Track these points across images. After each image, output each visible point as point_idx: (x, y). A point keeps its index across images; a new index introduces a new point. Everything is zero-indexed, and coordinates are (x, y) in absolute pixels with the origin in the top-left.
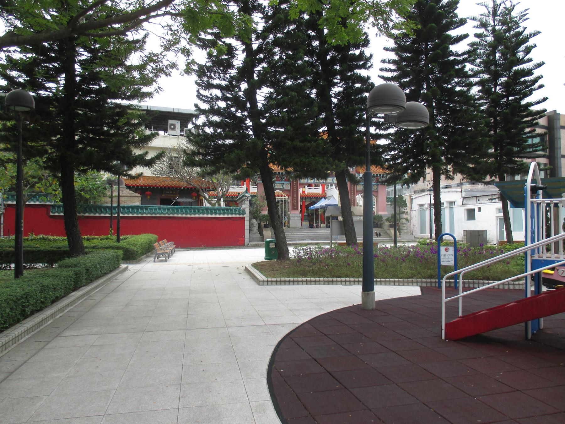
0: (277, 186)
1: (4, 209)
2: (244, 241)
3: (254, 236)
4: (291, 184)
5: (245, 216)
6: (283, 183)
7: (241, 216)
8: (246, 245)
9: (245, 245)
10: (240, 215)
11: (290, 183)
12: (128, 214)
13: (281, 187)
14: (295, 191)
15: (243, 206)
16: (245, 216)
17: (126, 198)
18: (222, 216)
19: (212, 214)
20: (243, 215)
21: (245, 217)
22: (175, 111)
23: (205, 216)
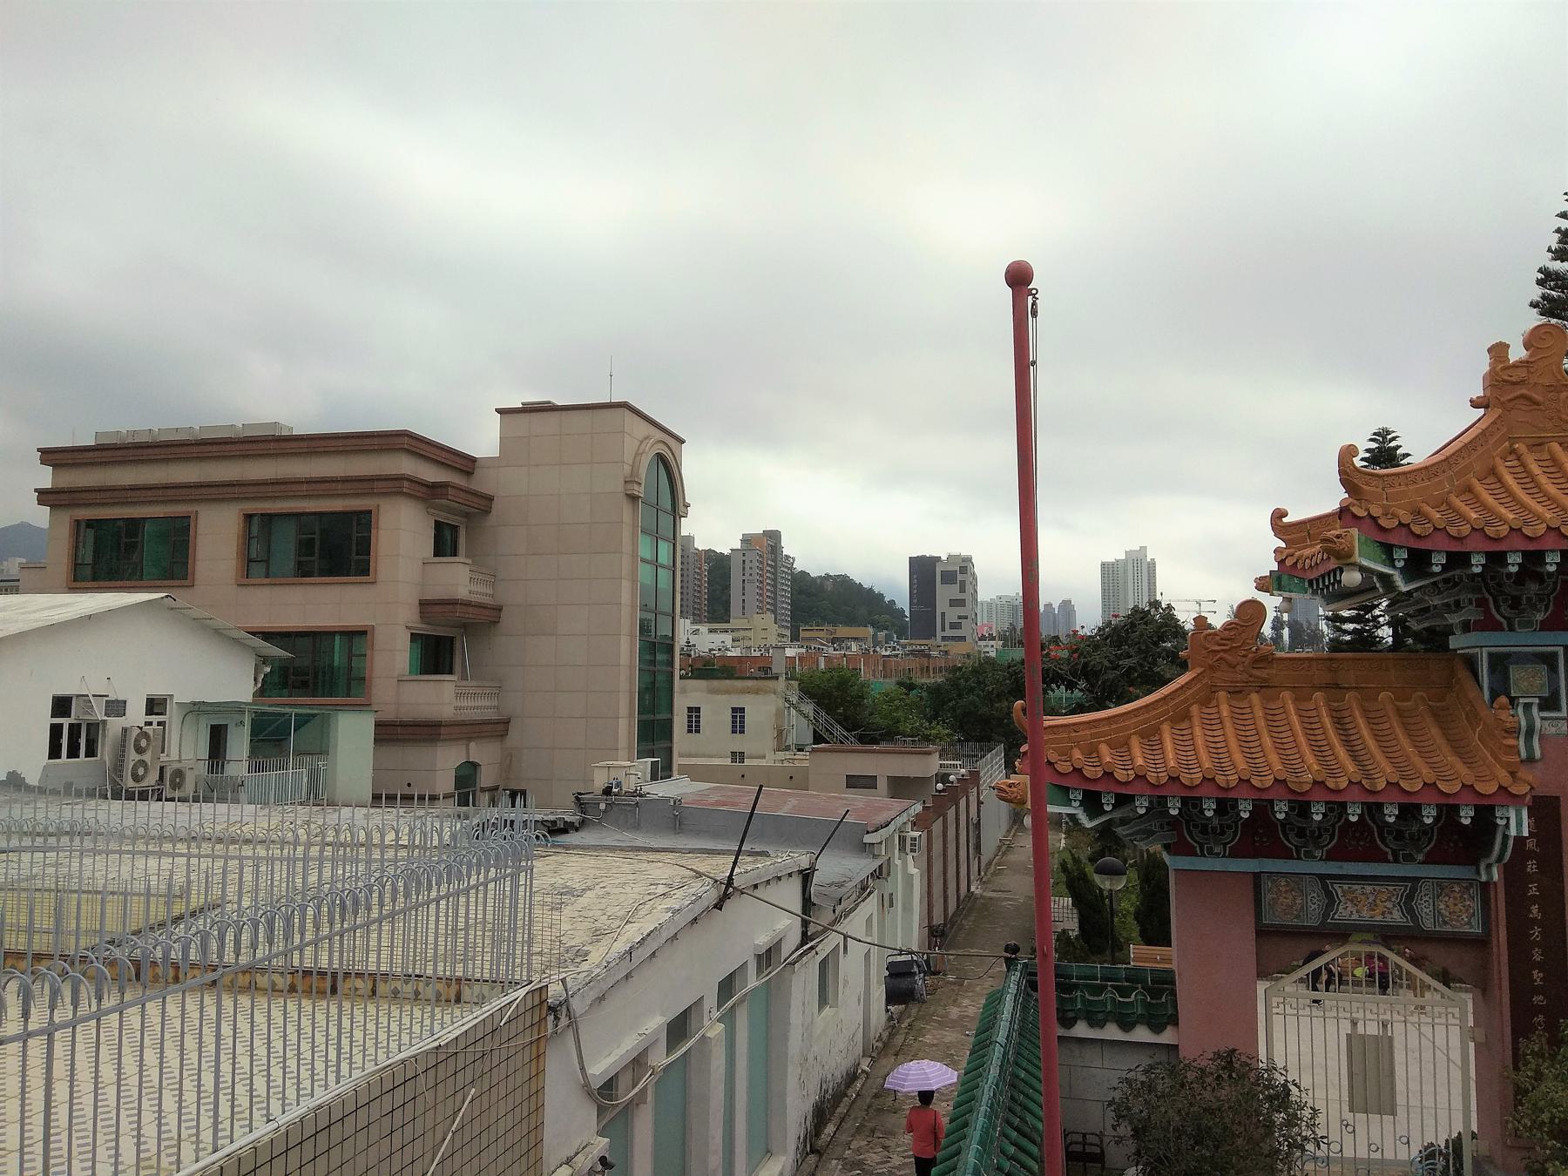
11: (1486, 887)
13: (1397, 917)
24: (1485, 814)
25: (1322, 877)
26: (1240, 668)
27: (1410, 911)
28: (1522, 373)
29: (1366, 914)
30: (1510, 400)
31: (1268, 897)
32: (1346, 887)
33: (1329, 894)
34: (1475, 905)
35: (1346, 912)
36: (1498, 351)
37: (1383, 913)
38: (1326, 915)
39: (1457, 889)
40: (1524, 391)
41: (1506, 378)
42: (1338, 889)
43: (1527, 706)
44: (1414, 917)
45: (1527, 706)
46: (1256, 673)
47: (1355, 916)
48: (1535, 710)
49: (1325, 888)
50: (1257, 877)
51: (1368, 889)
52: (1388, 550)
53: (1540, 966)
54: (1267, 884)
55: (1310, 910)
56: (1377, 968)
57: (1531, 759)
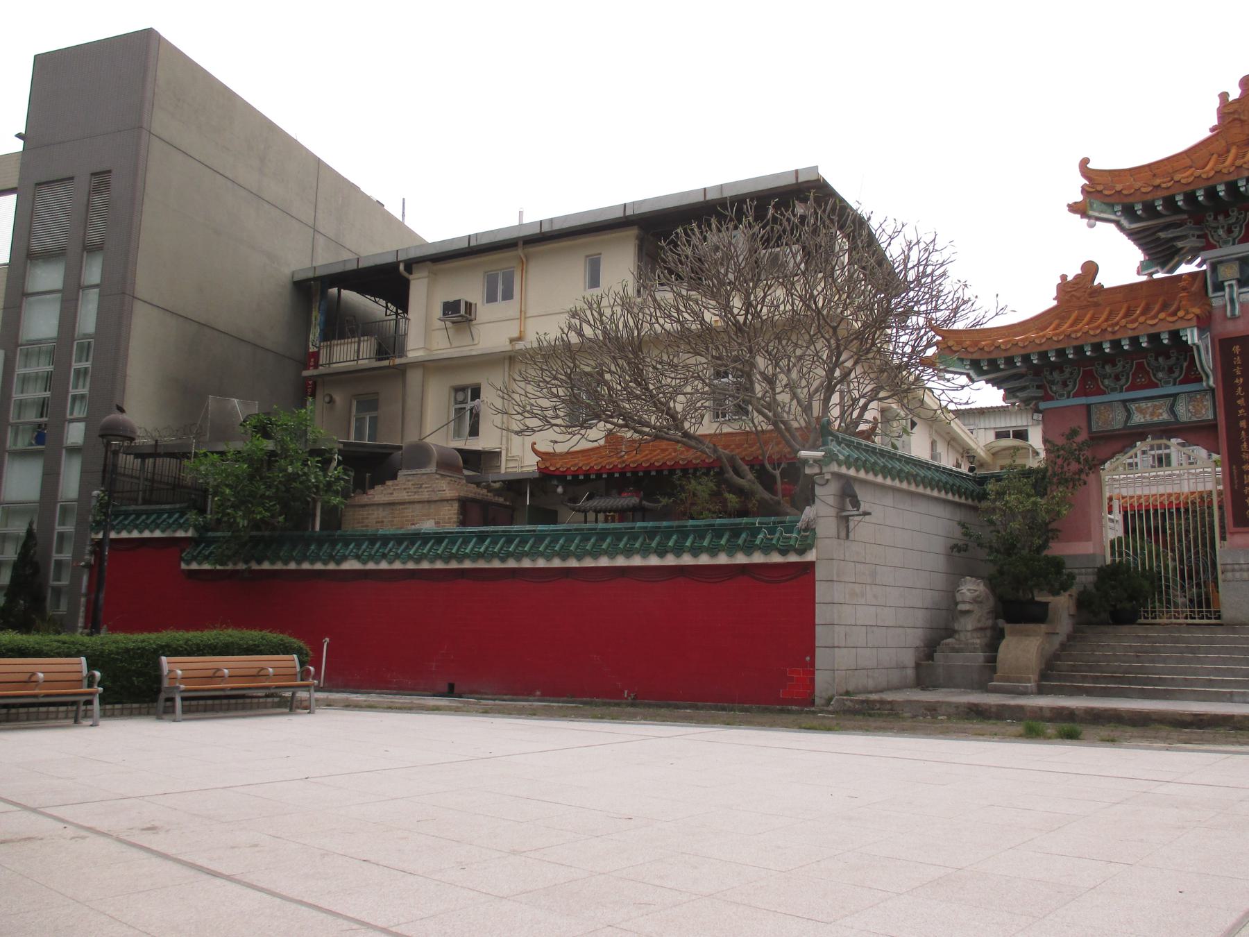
0: (1141, 411)
1: (91, 553)
2: (813, 681)
3: (958, 660)
4: (1220, 395)
5: (811, 556)
6: (1175, 396)
7: (793, 558)
8: (817, 700)
9: (813, 703)
10: (783, 552)
11: (1212, 390)
12: (377, 563)
13: (1165, 416)
14: (1243, 424)
15: (809, 512)
16: (811, 556)
17: (418, 506)
18: (704, 560)
19: (662, 554)
20: (801, 552)
21: (811, 566)
22: (709, 197)
23: (637, 561)
24: (1175, 335)
25: (1124, 402)
26: (1083, 298)
27: (1172, 411)
28: (1236, 106)
29: (1148, 418)
30: (1229, 122)
31: (1094, 417)
32: (1137, 405)
33: (1128, 411)
34: (1208, 403)
35: (1138, 419)
36: (1224, 96)
37: (1158, 416)
38: (1126, 421)
39: (1198, 397)
40: (1236, 116)
41: (1226, 111)
42: (1133, 406)
43: (1231, 286)
44: (1175, 416)
45: (1231, 286)
46: (1091, 300)
47: (1142, 420)
48: (1235, 288)
49: (1125, 407)
50: (1088, 406)
51: (1149, 404)
52: (1112, 206)
53: (1242, 429)
54: (1093, 409)
55: (1116, 420)
56: (1160, 452)
57: (1234, 317)
